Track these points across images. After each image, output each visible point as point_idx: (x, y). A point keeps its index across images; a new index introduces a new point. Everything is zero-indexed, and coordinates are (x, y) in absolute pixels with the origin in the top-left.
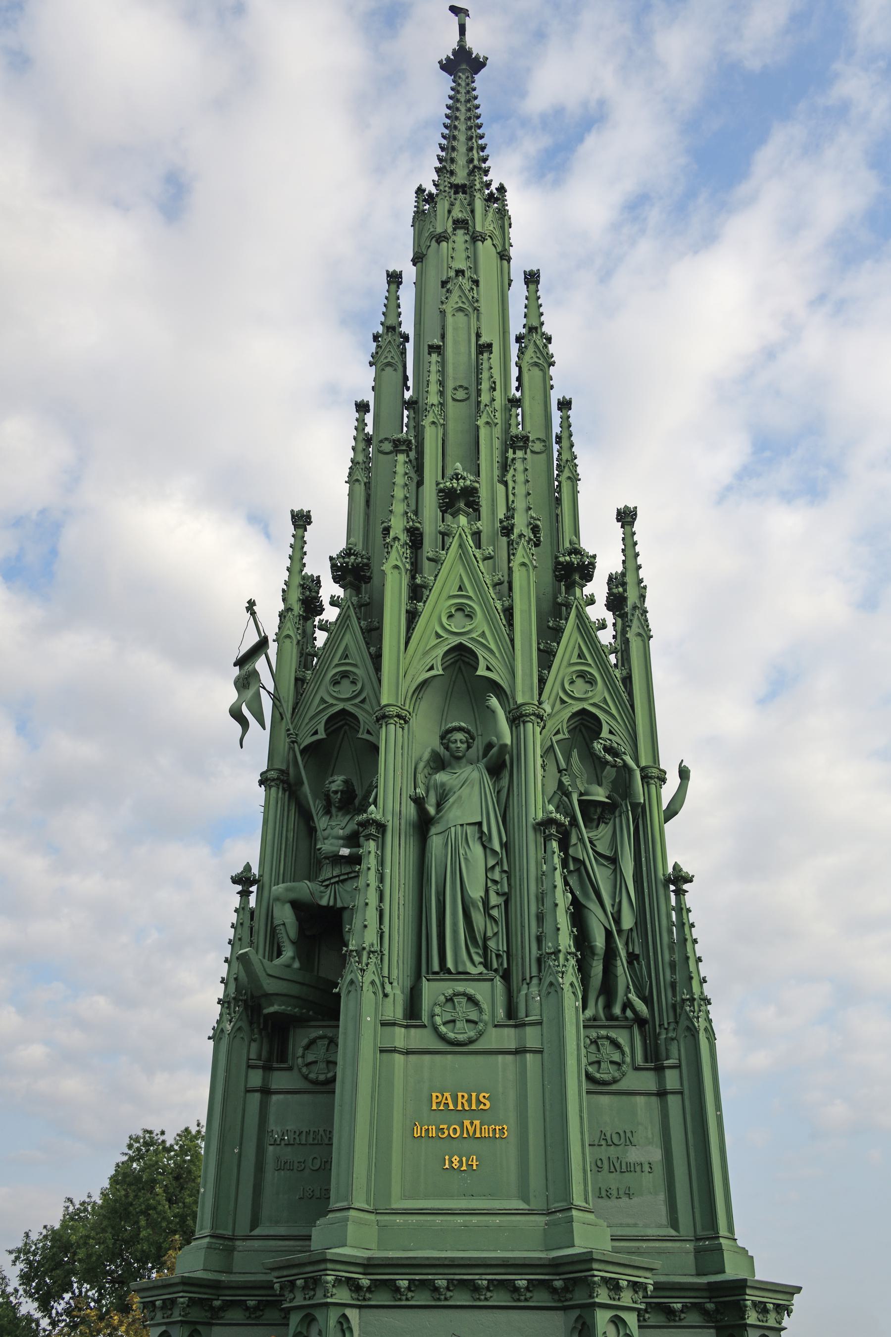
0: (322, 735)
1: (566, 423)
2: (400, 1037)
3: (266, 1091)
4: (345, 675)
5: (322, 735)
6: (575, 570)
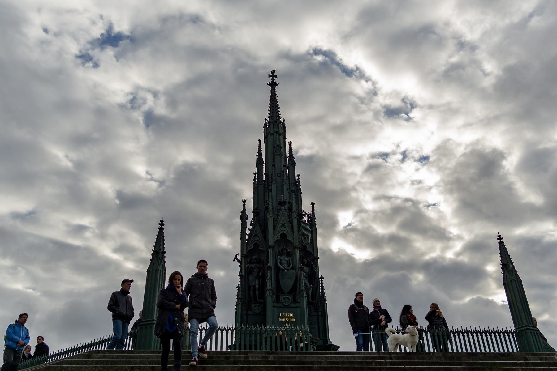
0: (252, 248)
1: (299, 179)
2: (276, 304)
3: (247, 315)
4: (256, 235)
5: (252, 248)
6: (301, 214)
